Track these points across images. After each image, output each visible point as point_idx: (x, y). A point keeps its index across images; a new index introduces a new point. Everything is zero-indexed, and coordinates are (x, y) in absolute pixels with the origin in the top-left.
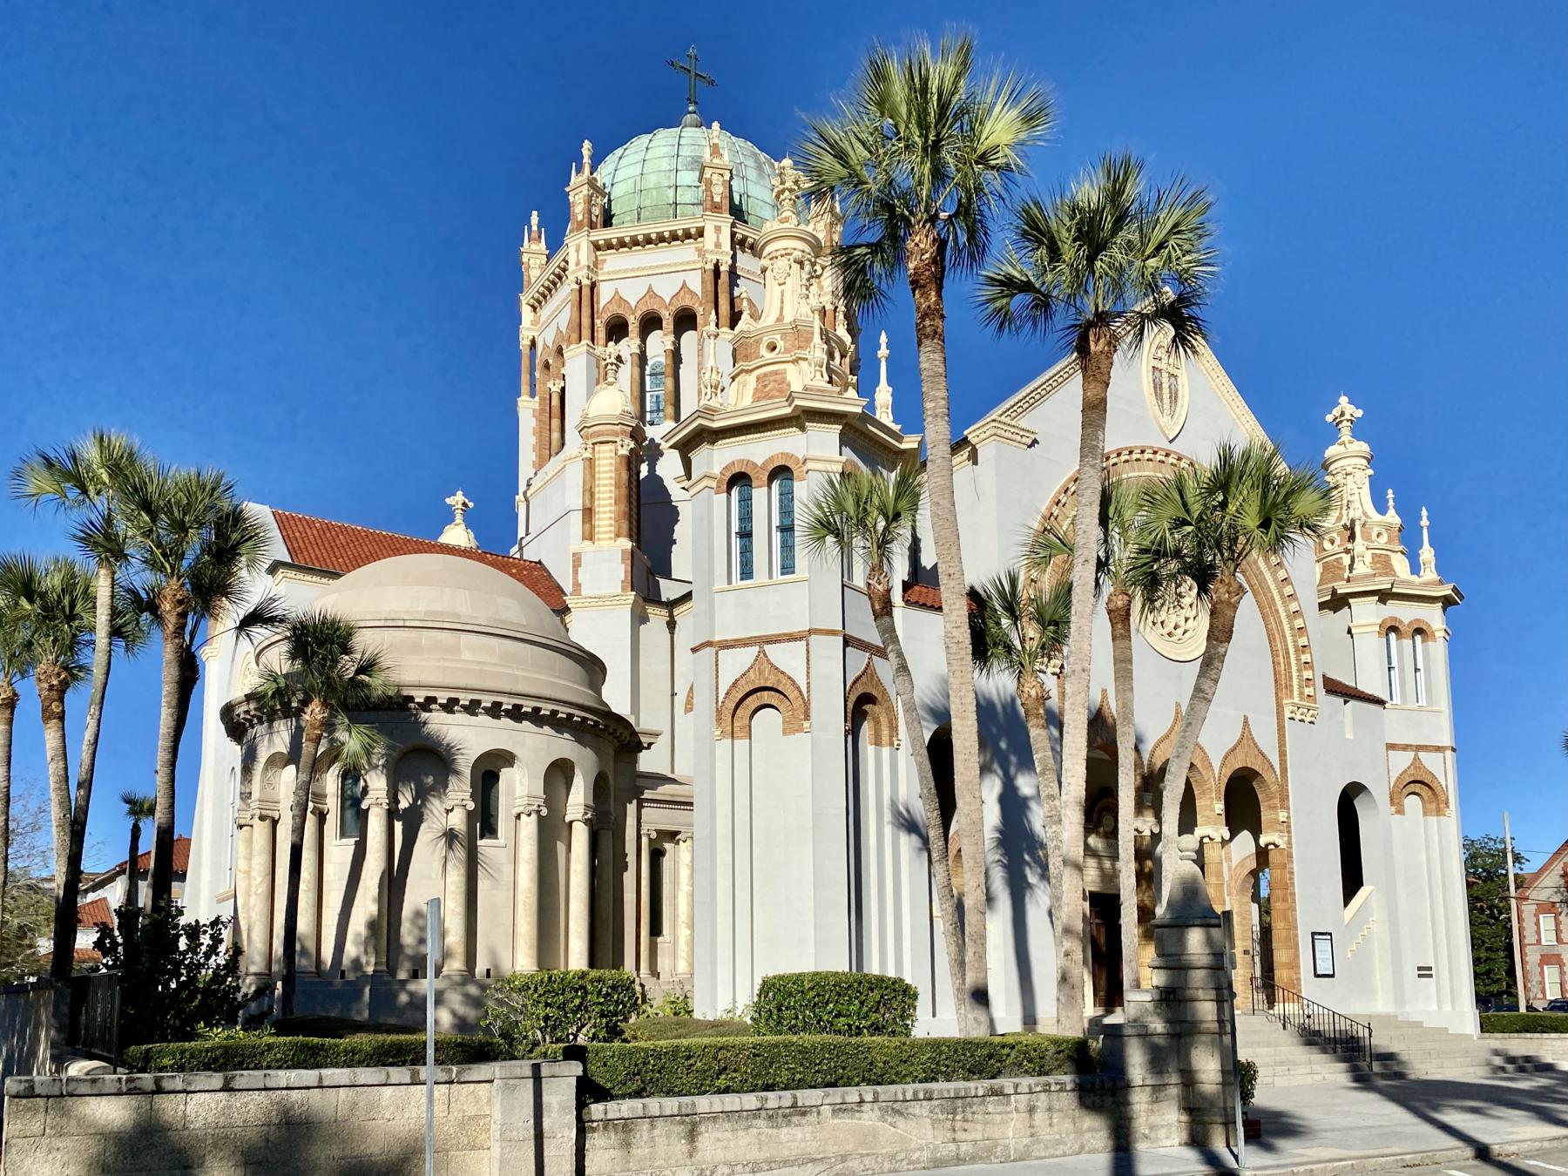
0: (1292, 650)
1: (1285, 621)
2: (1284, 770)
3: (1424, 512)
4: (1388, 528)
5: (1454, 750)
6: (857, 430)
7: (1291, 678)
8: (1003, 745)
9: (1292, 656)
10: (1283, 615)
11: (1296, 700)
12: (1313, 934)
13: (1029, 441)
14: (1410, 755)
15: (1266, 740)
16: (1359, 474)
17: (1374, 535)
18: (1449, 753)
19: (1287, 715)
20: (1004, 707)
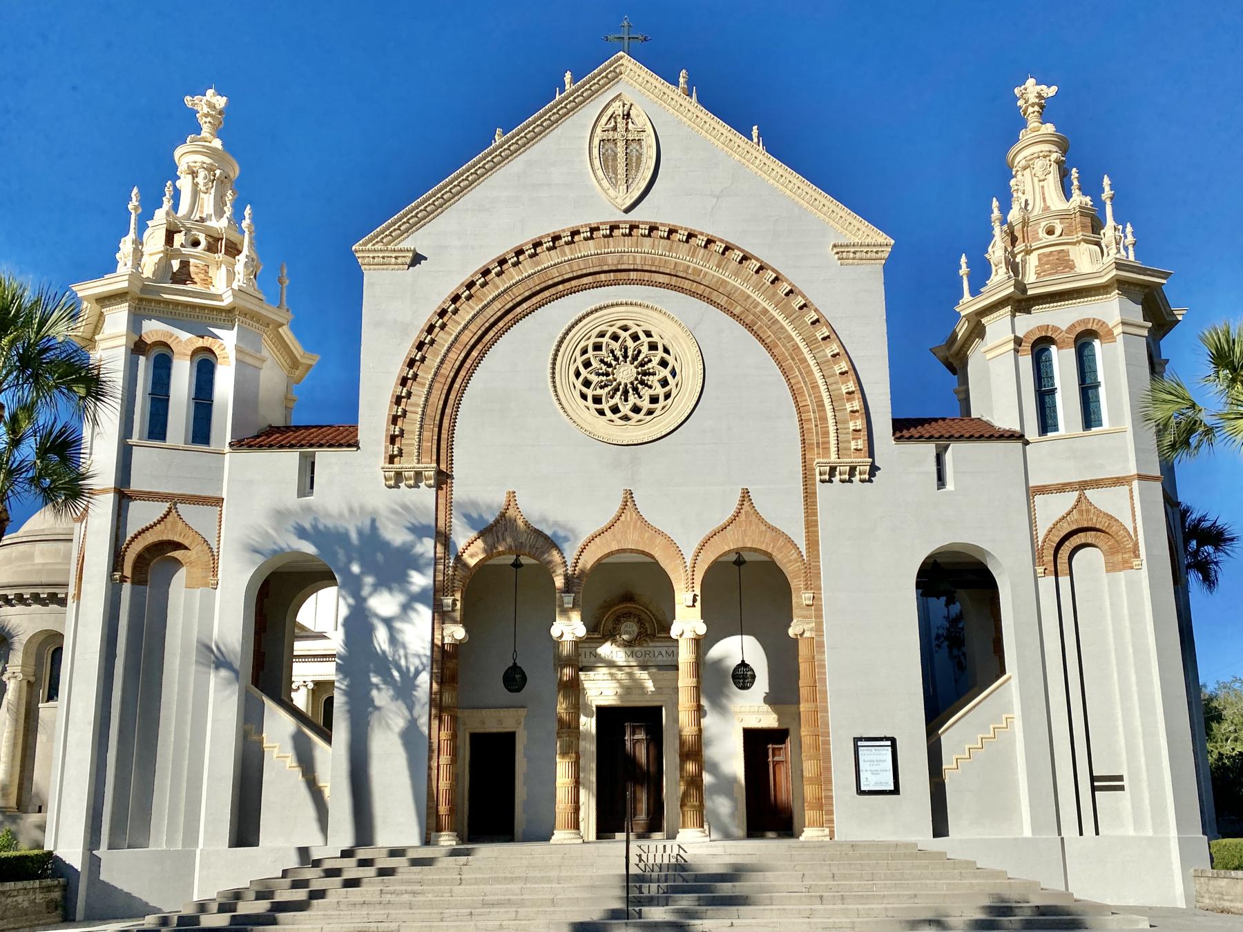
0: (827, 401)
1: (815, 369)
2: (812, 542)
3: (1106, 181)
4: (1063, 216)
5: (1141, 477)
6: (150, 301)
7: (826, 434)
8: (356, 569)
9: (828, 407)
10: (812, 362)
11: (833, 457)
12: (856, 740)
13: (408, 261)
14: (1071, 498)
15: (782, 511)
16: (1039, 164)
17: (1042, 234)
18: (1135, 483)
19: (818, 478)
20: (360, 533)
